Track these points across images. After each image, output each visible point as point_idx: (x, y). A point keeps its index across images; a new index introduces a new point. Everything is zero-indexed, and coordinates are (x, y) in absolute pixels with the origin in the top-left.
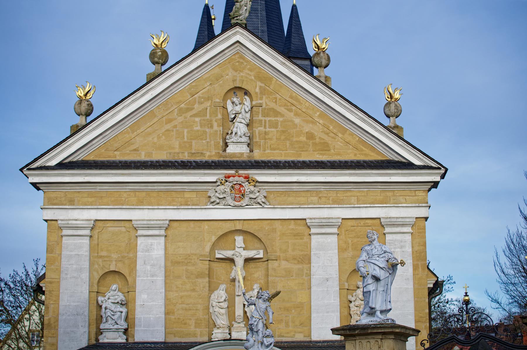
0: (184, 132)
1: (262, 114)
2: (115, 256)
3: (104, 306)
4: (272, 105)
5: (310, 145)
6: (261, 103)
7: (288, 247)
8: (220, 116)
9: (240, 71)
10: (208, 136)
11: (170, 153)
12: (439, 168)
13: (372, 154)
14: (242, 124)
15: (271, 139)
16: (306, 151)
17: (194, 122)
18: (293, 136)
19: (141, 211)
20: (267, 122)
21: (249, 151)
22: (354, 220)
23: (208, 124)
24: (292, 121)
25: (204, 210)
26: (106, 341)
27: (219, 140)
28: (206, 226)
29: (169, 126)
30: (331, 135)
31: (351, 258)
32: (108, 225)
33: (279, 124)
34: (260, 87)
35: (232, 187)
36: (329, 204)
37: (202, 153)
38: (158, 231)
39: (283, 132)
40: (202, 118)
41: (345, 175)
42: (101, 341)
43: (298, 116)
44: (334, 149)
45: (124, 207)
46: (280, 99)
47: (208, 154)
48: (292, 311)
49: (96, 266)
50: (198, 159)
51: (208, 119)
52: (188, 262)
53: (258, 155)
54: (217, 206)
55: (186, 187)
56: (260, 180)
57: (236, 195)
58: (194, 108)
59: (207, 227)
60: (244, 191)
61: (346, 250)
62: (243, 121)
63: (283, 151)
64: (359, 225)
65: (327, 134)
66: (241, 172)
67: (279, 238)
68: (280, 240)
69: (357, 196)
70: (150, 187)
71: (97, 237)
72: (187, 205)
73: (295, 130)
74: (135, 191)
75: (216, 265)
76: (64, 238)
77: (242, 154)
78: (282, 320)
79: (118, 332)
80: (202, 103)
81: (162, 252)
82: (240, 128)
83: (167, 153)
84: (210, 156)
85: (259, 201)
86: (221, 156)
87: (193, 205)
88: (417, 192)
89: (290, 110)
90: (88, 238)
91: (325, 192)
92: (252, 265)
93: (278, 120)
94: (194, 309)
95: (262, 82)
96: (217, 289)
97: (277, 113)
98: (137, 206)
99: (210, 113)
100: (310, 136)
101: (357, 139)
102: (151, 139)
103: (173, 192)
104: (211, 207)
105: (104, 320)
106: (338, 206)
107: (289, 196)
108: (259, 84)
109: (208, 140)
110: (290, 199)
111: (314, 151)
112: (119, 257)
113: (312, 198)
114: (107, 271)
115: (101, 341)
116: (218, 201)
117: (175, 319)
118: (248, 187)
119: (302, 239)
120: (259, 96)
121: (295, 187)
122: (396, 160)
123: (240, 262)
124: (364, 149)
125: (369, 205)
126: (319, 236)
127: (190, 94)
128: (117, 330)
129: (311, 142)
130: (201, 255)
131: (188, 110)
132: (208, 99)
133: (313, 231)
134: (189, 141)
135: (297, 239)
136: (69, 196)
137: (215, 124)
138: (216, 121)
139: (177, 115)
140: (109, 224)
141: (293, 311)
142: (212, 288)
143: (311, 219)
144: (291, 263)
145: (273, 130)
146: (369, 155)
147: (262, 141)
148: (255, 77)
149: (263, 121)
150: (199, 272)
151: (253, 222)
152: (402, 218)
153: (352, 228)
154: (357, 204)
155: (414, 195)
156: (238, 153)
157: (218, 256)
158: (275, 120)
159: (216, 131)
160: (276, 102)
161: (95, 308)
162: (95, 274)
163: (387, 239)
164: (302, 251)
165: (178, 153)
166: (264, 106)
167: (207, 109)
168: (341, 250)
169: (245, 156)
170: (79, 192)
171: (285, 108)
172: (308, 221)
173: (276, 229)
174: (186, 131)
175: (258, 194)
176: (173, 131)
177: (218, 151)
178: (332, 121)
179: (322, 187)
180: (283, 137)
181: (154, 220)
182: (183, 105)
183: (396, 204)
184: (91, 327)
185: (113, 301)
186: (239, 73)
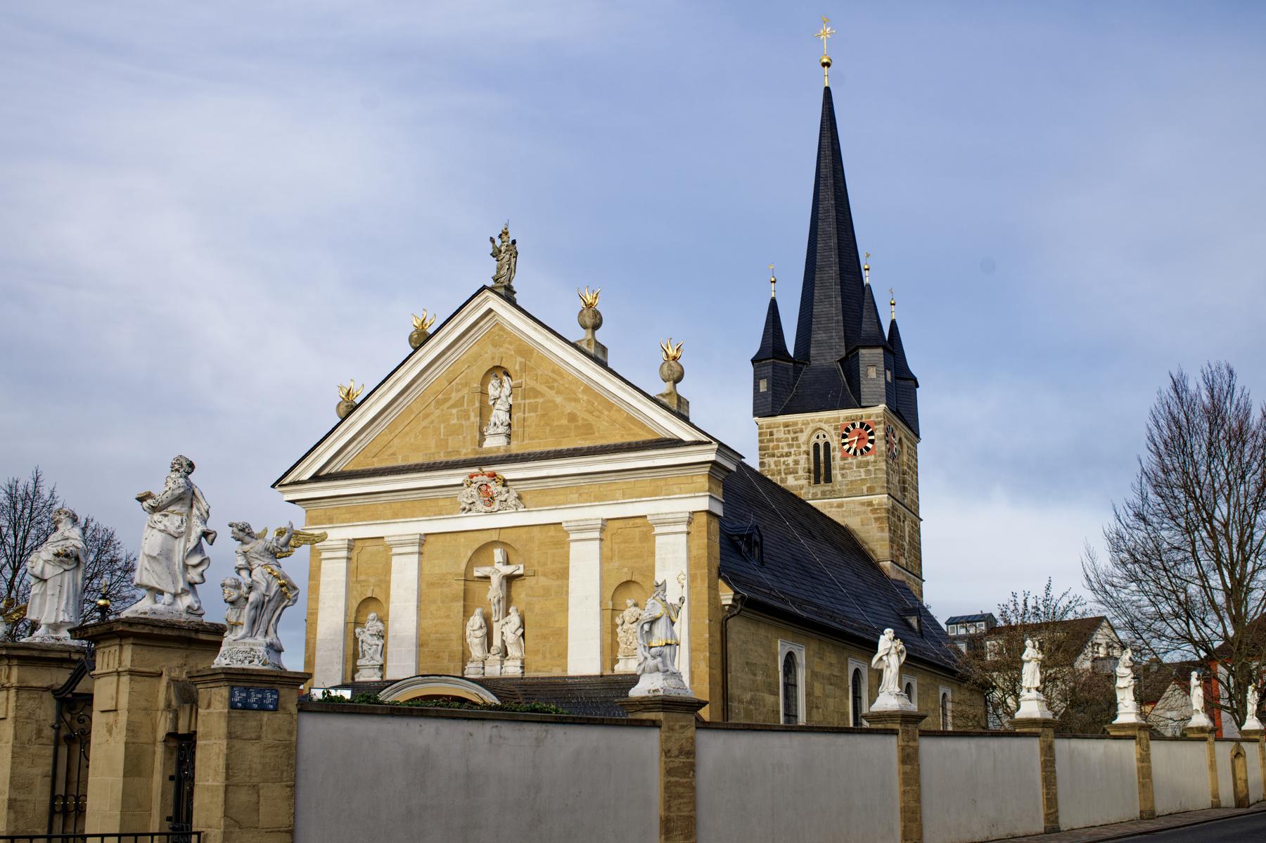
0: (440, 428)
1: (521, 396)
2: (372, 580)
3: (360, 639)
4: (532, 384)
5: (571, 429)
6: (519, 383)
7: (547, 559)
8: (477, 404)
9: (500, 346)
10: (465, 431)
11: (426, 454)
12: (710, 443)
13: (642, 433)
16: (568, 437)
17: (451, 414)
18: (553, 420)
19: (396, 525)
20: (527, 406)
21: (506, 444)
23: (465, 416)
24: (553, 402)
25: (457, 520)
26: (362, 679)
27: (475, 434)
28: (462, 537)
29: (425, 423)
30: (596, 413)
32: (367, 545)
33: (539, 405)
34: (521, 363)
35: (480, 489)
36: (591, 502)
37: (458, 451)
38: (412, 547)
39: (543, 415)
40: (459, 409)
41: (600, 462)
42: (357, 680)
43: (560, 394)
44: (599, 432)
45: (378, 522)
46: (541, 375)
47: (464, 451)
48: (549, 638)
49: (355, 592)
50: (454, 458)
51: (465, 409)
52: (443, 584)
53: (516, 448)
54: (469, 514)
55: (438, 493)
56: (507, 478)
58: (450, 398)
59: (463, 540)
61: (612, 559)
62: (502, 408)
65: (591, 413)
66: (486, 469)
67: (537, 549)
68: (538, 550)
69: (623, 489)
70: (402, 496)
71: (356, 558)
72: (441, 514)
73: (556, 412)
74: (390, 502)
75: (478, 585)
76: (323, 562)
77: (498, 448)
78: (538, 650)
79: (374, 668)
80: (459, 391)
81: (415, 573)
82: (499, 415)
83: (423, 455)
84: (466, 454)
86: (477, 453)
87: (447, 514)
88: (694, 478)
89: (551, 388)
90: (345, 560)
92: (517, 585)
93: (538, 402)
94: (448, 639)
95: (522, 357)
96: (471, 616)
97: (537, 394)
98: (392, 519)
99: (468, 403)
101: (625, 415)
102: (407, 440)
103: (428, 501)
104: (463, 514)
105: (361, 655)
106: (598, 503)
108: (519, 359)
109: (464, 435)
110: (548, 499)
111: (576, 436)
112: (376, 581)
113: (572, 496)
114: (365, 597)
115: (357, 680)
116: (467, 507)
117: (429, 651)
118: (495, 488)
119: (563, 548)
120: (519, 374)
121: (550, 483)
122: (668, 437)
123: (495, 580)
124: (633, 427)
125: (634, 500)
126: (579, 543)
127: (447, 381)
128: (373, 667)
129: (573, 424)
130: (456, 575)
131: (446, 400)
132: (466, 384)
133: (573, 536)
134: (446, 438)
135: (557, 548)
136: (328, 513)
138: (473, 411)
139: (434, 407)
140: (369, 543)
141: (551, 639)
142: (467, 614)
143: (567, 522)
144: (550, 579)
145: (531, 414)
146: (638, 434)
147: (520, 429)
149: (522, 405)
150: (454, 594)
151: (510, 530)
152: (672, 513)
153: (619, 531)
154: (624, 499)
155: (691, 481)
158: (535, 402)
159: (473, 423)
160: (536, 380)
161: (352, 641)
162: (354, 601)
164: (562, 563)
165: (435, 453)
166: (523, 386)
167: (464, 397)
168: (604, 559)
169: (502, 448)
170: (338, 508)
171: (547, 386)
172: (564, 525)
173: (534, 537)
174: (442, 425)
175: (507, 495)
176: (429, 427)
177: (474, 447)
178: (597, 395)
179: (581, 481)
180: (543, 422)
181: (404, 535)
182: (440, 395)
184: (348, 663)
185: (371, 632)
186: (498, 349)
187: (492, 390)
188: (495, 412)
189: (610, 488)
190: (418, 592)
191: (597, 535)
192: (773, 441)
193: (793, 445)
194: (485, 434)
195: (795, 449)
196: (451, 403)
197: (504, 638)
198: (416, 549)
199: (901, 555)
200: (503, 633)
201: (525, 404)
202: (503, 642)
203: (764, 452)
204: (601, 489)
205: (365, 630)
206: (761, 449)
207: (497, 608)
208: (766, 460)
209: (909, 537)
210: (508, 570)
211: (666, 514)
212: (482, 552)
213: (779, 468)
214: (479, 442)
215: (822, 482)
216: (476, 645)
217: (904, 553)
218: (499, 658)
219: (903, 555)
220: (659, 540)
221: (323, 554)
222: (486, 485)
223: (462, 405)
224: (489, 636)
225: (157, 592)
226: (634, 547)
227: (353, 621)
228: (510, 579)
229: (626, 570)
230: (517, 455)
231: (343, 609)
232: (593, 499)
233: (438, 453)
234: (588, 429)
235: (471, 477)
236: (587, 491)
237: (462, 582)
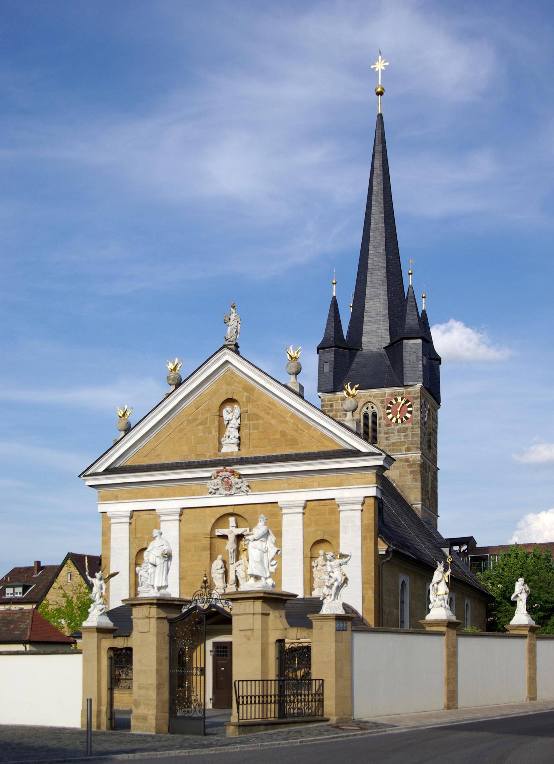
1: (247, 419)
6: (246, 410)
14: (233, 429)
15: (253, 439)
21: (237, 450)
22: (316, 502)
31: (314, 532)
36: (297, 489)
39: (263, 432)
41: (306, 465)
57: (226, 486)
60: (231, 482)
63: (262, 448)
64: (321, 505)
69: (318, 481)
77: (232, 453)
85: (243, 490)
86: (217, 455)
91: (294, 479)
93: (259, 423)
96: (216, 559)
100: (283, 434)
107: (266, 484)
119: (277, 518)
123: (232, 538)
129: (284, 438)
137: (213, 430)
142: (212, 559)
145: (255, 431)
148: (242, 389)
149: (248, 425)
152: (352, 497)
154: (318, 487)
156: (230, 452)
157: (217, 533)
158: (257, 423)
163: (341, 515)
166: (249, 412)
168: (305, 525)
169: (235, 454)
183: (350, 486)
187: (226, 416)
188: (229, 429)
189: (310, 480)
190: (179, 545)
191: (301, 510)
194: (222, 443)
196: (199, 422)
197: (237, 574)
198: (177, 517)
199: (427, 499)
200: (236, 571)
201: (250, 424)
202: (236, 577)
204: (304, 481)
205: (141, 568)
207: (232, 555)
209: (431, 484)
210: (239, 531)
211: (348, 498)
212: (222, 519)
214: (219, 448)
216: (219, 579)
217: (428, 497)
218: (234, 586)
219: (428, 498)
220: (342, 514)
221: (112, 520)
222: (228, 478)
223: (206, 424)
224: (226, 573)
225: (257, 578)
226: (325, 518)
227: (135, 563)
228: (240, 537)
229: (320, 532)
230: (247, 458)
231: (128, 555)
232: (298, 488)
233: (191, 455)
234: (294, 442)
235: (218, 472)
236: (294, 482)
237: (209, 539)
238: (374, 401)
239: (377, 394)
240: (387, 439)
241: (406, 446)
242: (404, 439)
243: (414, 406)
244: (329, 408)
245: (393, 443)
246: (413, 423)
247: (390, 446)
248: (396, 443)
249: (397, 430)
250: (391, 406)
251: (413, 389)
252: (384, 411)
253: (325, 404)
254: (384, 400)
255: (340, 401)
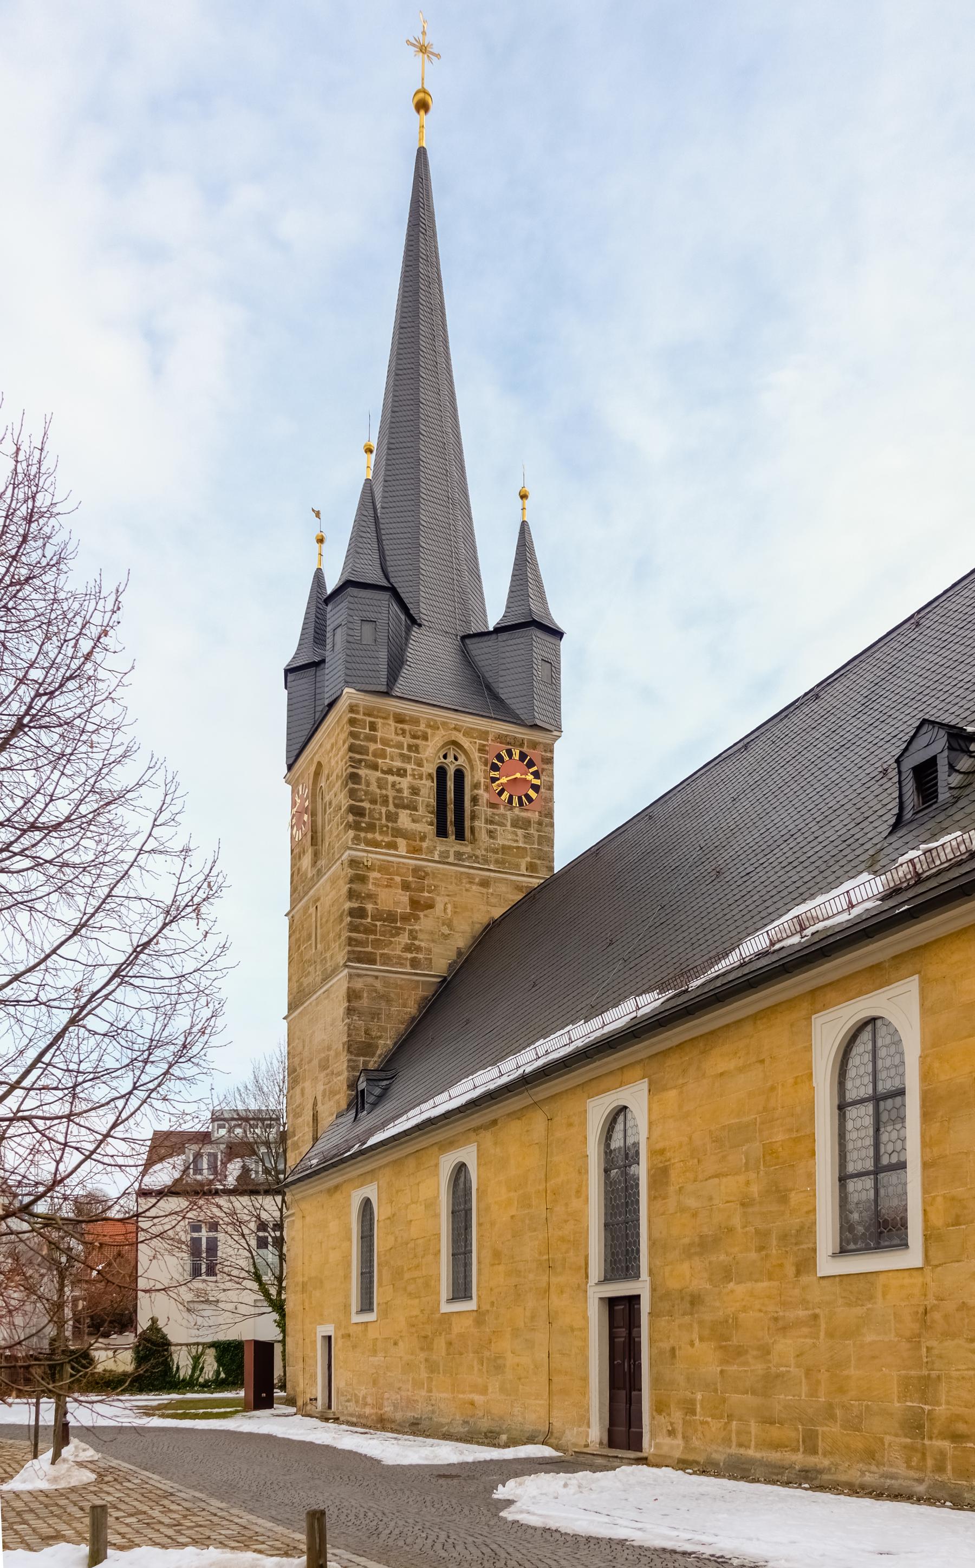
192: (376, 742)
193: (409, 758)
195: (536, 834)
203: (358, 756)
206: (352, 749)
208: (362, 772)
213: (384, 792)
215: (452, 837)
238: (465, 742)
239: (472, 729)
240: (491, 834)
241: (528, 859)
242: (525, 843)
243: (543, 778)
244: (367, 731)
245: (504, 847)
246: (540, 812)
247: (497, 853)
248: (510, 848)
249: (512, 820)
250: (499, 764)
251: (541, 740)
252: (485, 771)
253: (358, 720)
254: (484, 745)
255: (391, 722)
